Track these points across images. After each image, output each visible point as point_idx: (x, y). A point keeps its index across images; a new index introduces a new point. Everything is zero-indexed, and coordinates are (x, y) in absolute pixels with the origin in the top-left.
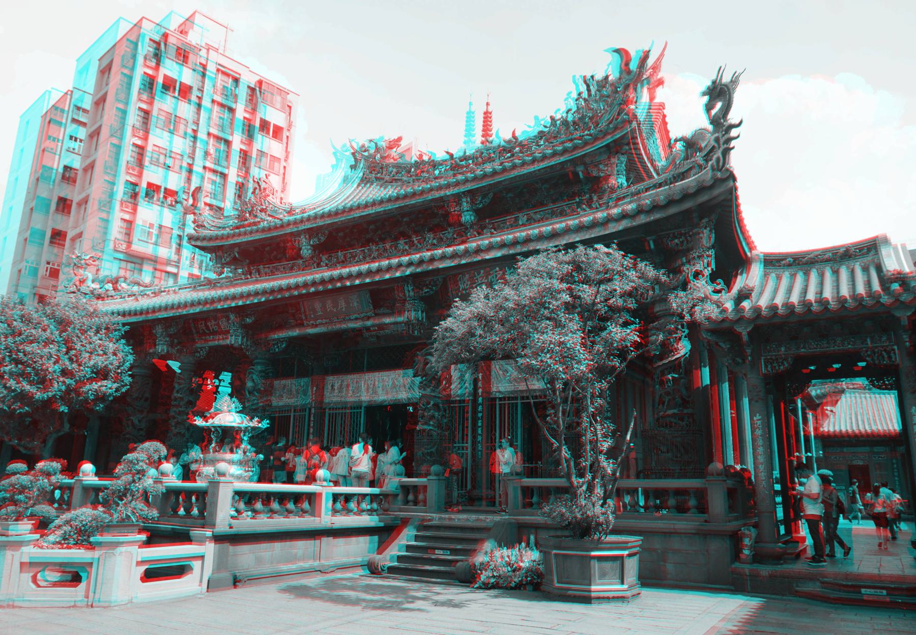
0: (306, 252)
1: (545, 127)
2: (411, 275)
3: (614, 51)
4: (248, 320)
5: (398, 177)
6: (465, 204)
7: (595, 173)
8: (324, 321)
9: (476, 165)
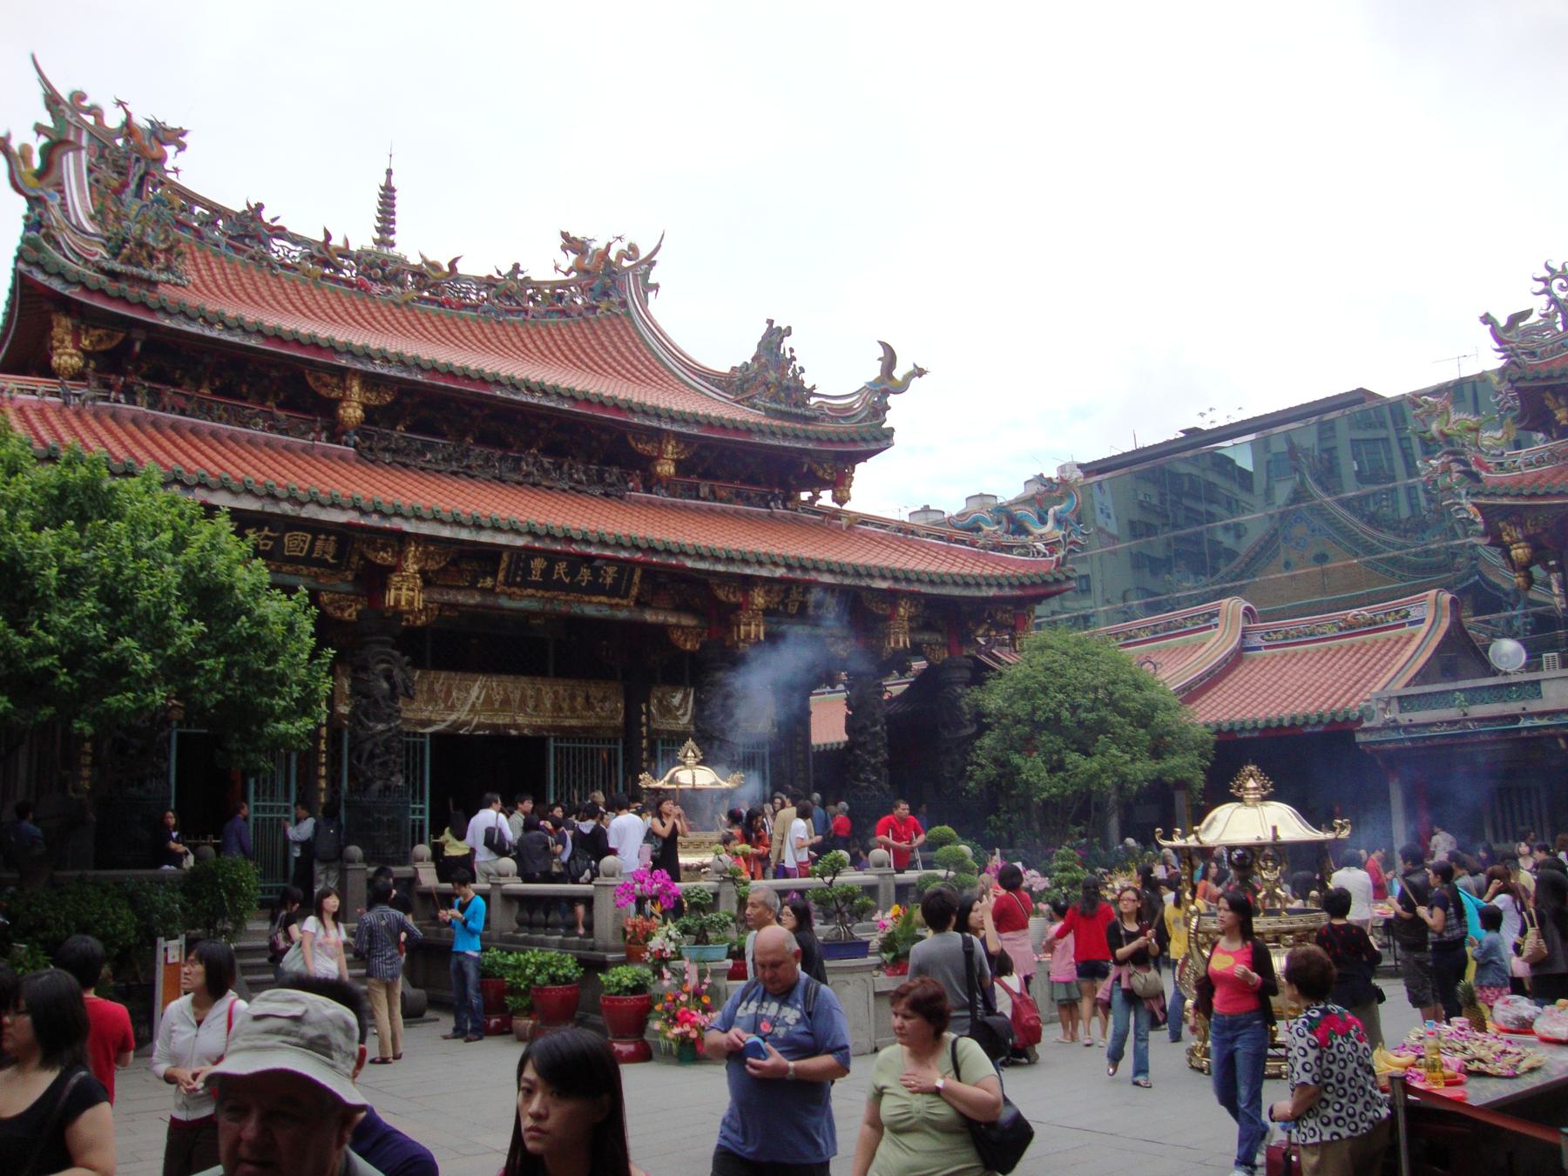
0: (352, 412)
2: (781, 580)
3: (881, 343)
4: (432, 566)
7: (820, 473)
8: (540, 593)
9: (370, 278)
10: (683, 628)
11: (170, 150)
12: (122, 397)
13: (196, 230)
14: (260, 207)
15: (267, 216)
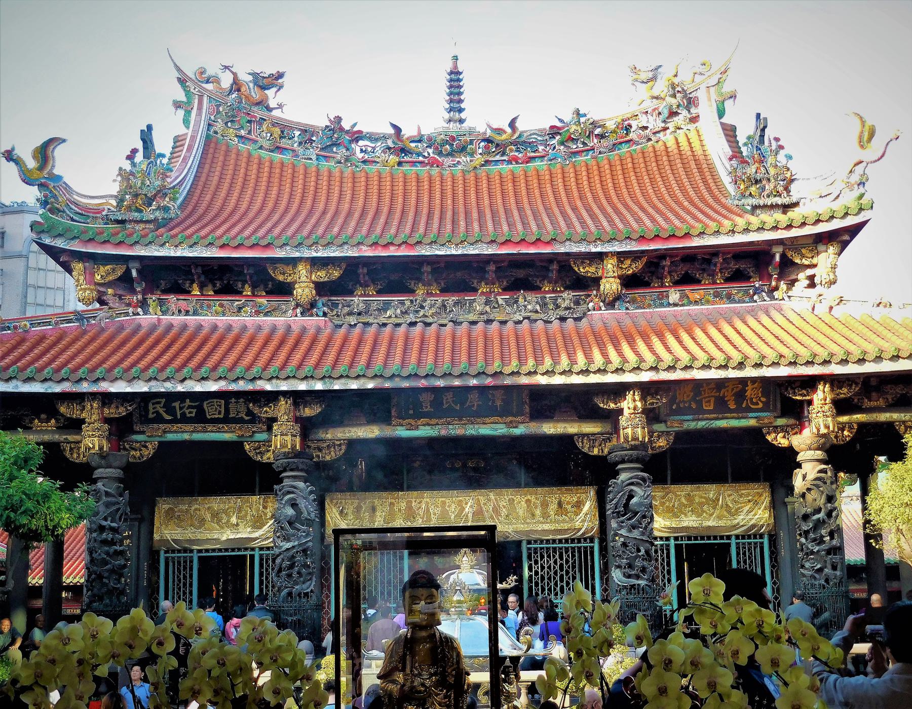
0: (304, 291)
1: (561, 120)
5: (284, 143)
6: (610, 266)
8: (434, 421)
9: (440, 154)
10: (587, 435)
11: (270, 93)
12: (139, 310)
13: (294, 151)
14: (339, 119)
15: (346, 125)
